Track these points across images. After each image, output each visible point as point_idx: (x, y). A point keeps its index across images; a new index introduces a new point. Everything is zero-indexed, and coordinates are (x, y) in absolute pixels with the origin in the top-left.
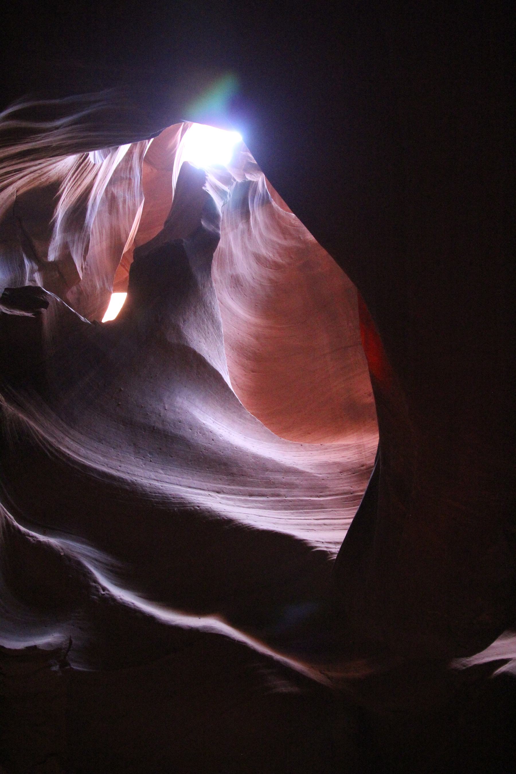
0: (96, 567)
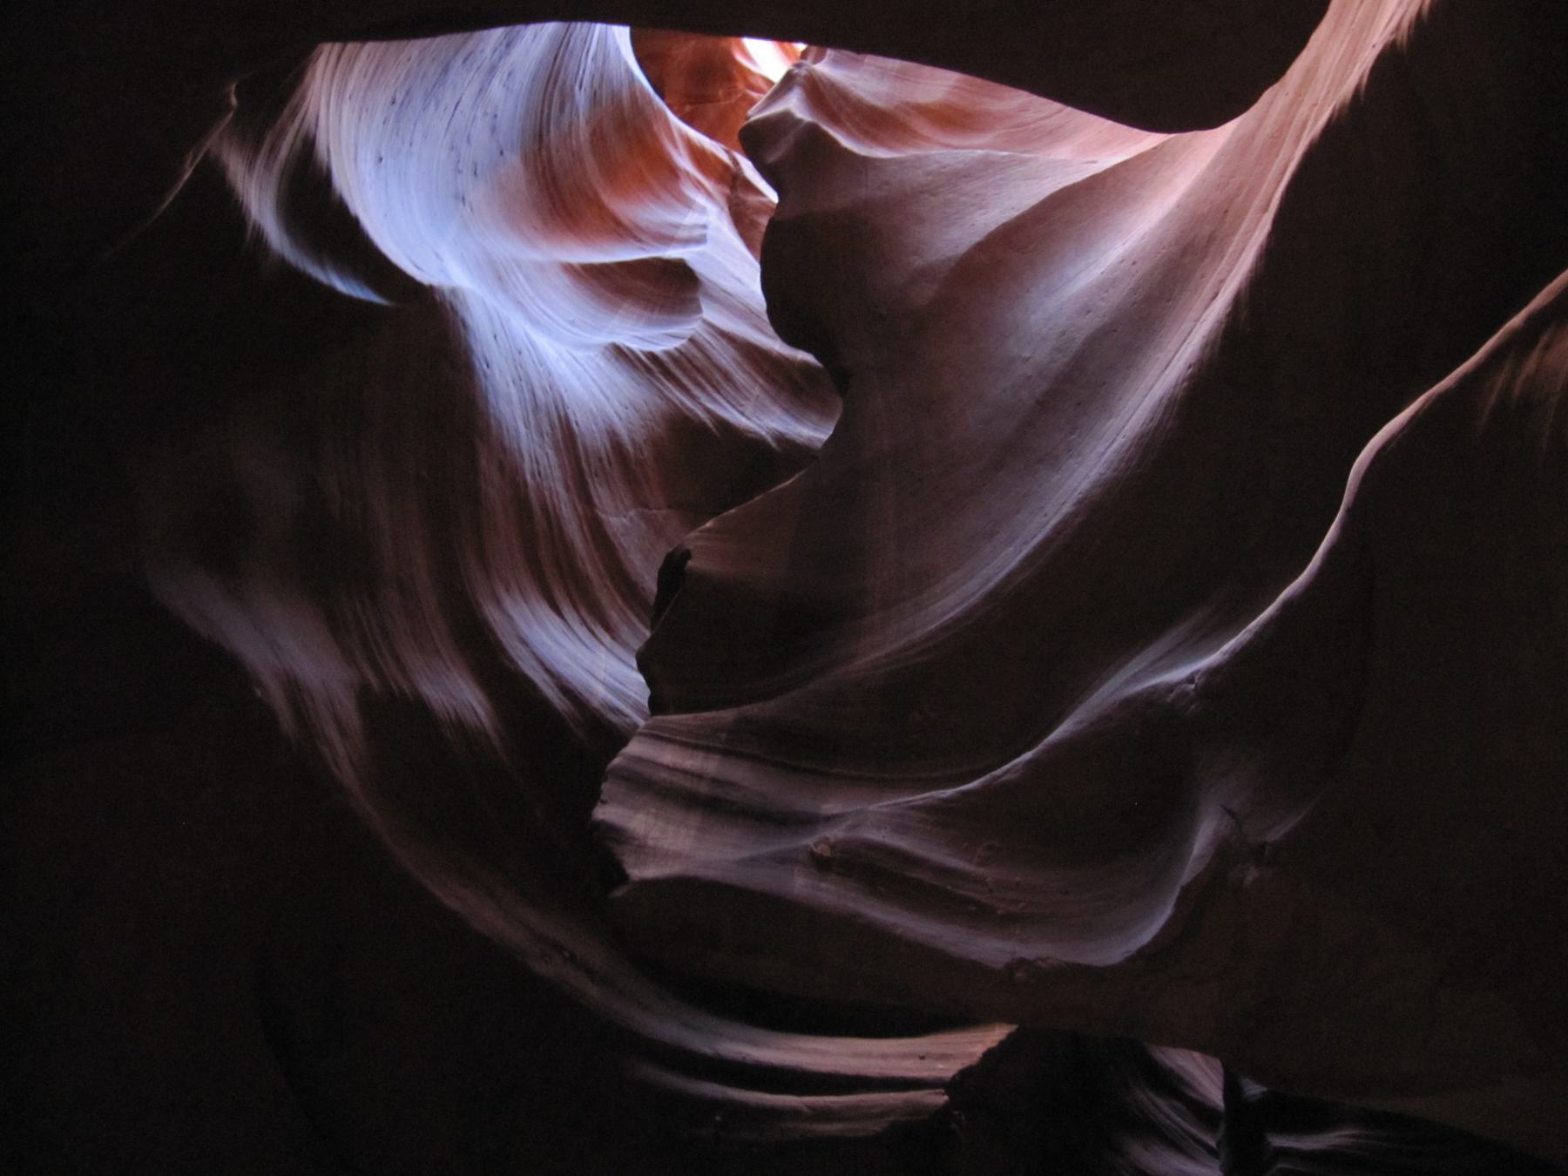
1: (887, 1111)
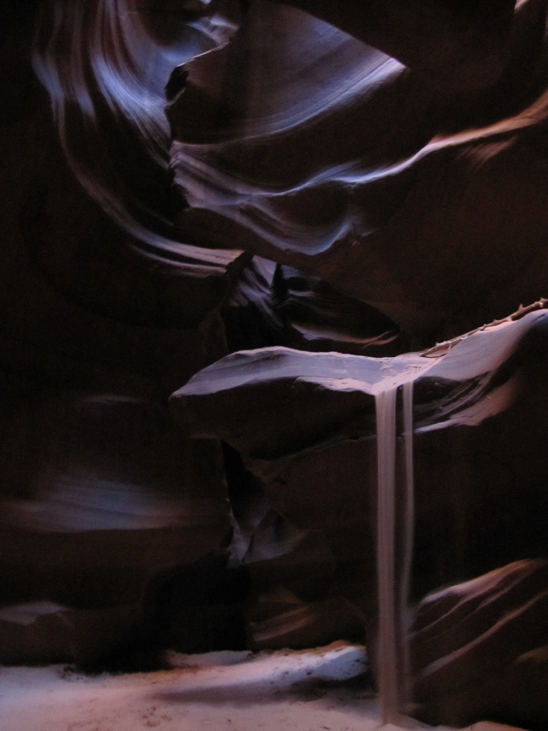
0: (345, 176)
1: (207, 272)
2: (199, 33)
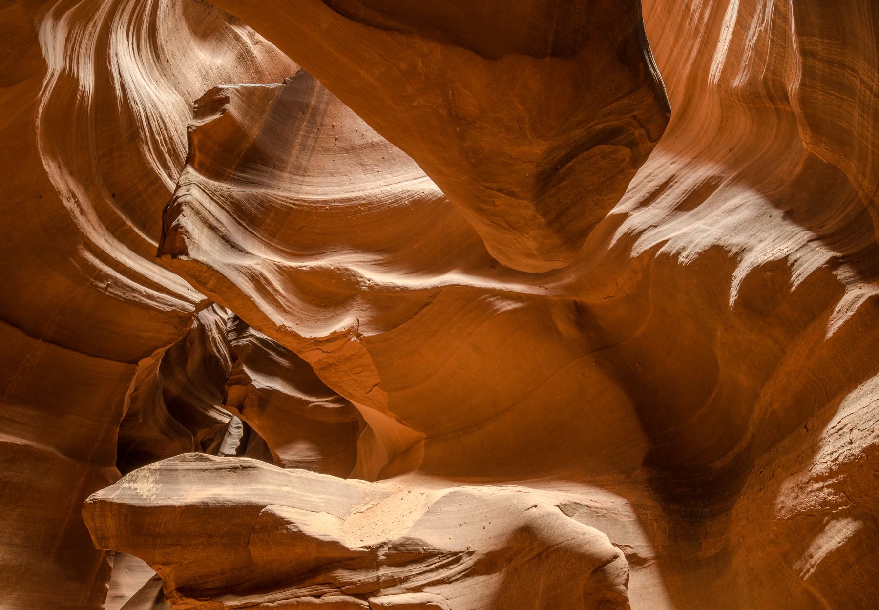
0: (362, 267)
2: (237, 38)
